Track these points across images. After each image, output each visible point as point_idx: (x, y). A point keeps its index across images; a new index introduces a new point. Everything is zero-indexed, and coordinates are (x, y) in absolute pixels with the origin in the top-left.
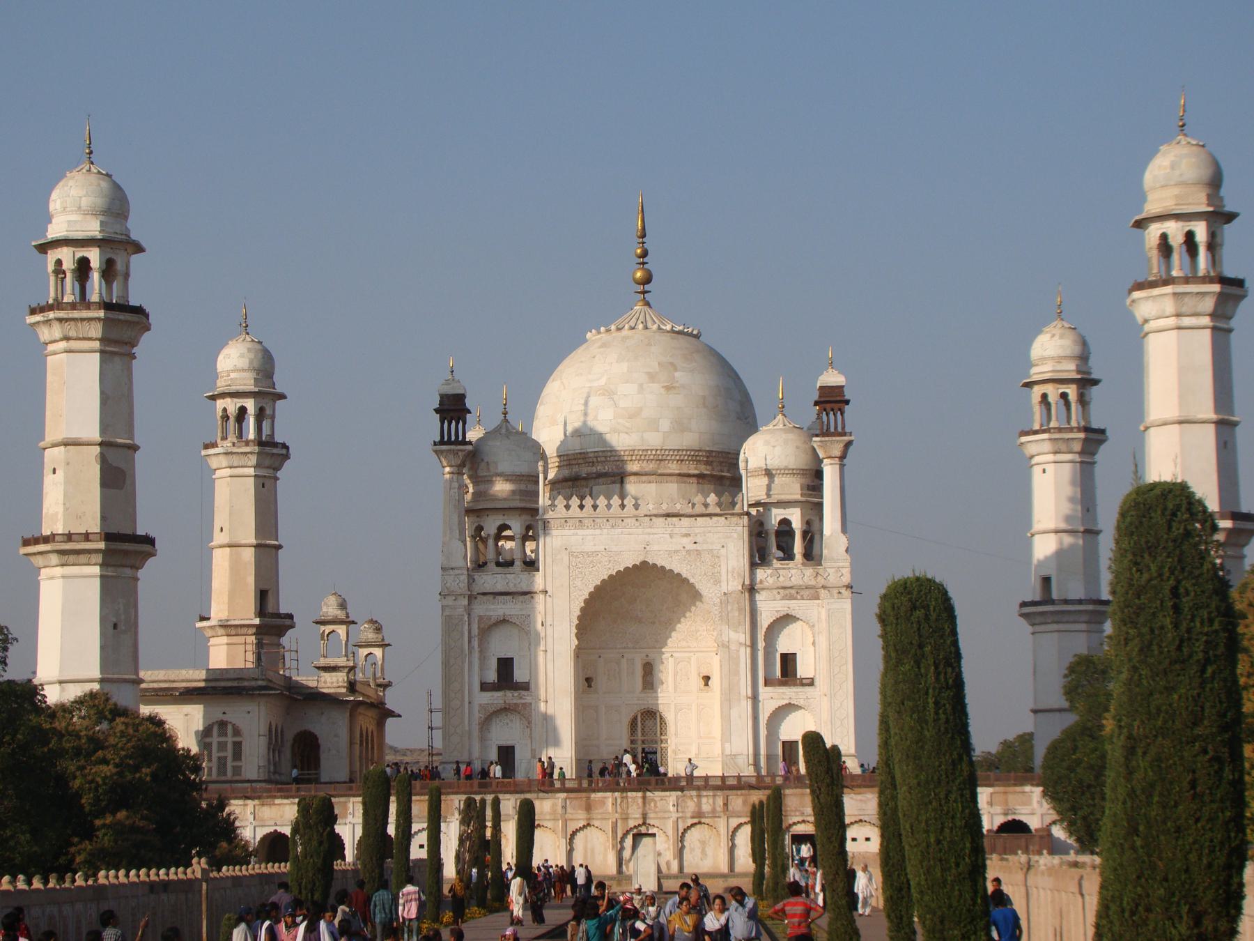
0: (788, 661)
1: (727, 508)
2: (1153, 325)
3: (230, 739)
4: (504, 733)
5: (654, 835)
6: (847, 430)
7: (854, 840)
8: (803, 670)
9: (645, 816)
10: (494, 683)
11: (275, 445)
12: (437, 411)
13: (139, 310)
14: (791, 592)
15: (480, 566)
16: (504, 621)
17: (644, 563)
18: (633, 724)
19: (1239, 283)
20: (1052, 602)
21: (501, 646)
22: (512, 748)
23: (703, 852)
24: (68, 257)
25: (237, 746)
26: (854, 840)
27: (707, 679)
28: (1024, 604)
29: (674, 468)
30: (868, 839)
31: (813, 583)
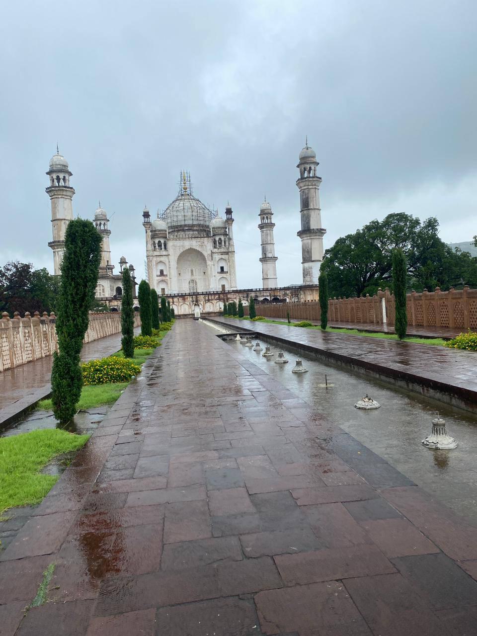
0: (222, 268)
1: (208, 236)
2: (302, 188)
3: (101, 288)
4: (163, 286)
9: (197, 301)
11: (108, 230)
13: (72, 188)
14: (222, 253)
15: (155, 250)
18: (190, 282)
19: (320, 178)
20: (266, 258)
21: (161, 267)
22: (164, 289)
23: (210, 308)
24: (55, 176)
25: (103, 289)
27: (204, 273)
28: (260, 259)
29: (195, 228)
31: (227, 251)
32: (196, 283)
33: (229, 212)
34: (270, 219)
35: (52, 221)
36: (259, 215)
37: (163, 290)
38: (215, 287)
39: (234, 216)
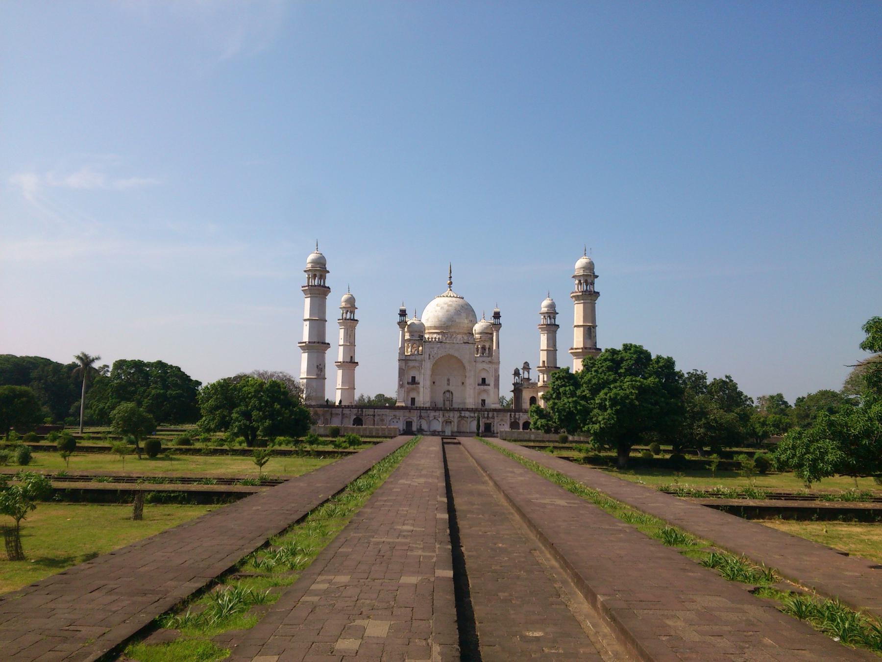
0: (484, 380)
8: (487, 382)
33: (497, 316)
39: (502, 320)
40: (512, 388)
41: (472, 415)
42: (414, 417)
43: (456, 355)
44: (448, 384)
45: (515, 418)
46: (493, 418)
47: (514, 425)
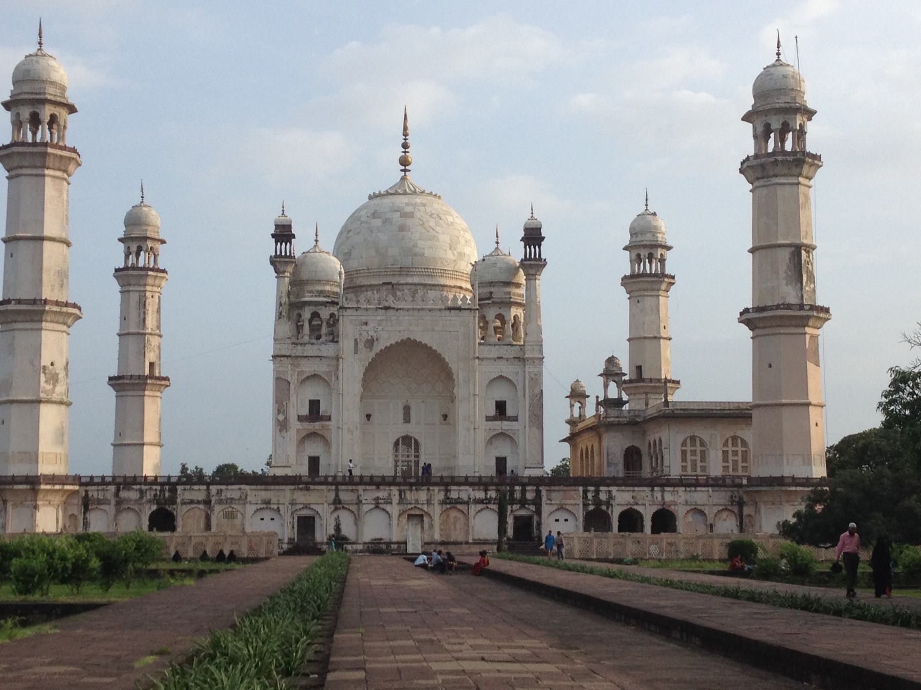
0: (501, 407)
4: (314, 449)
5: (422, 516)
6: (543, 257)
7: (557, 520)
8: (510, 412)
10: (306, 416)
12: (273, 236)
16: (315, 376)
17: (409, 339)
18: (396, 444)
21: (313, 392)
26: (557, 520)
27: (445, 417)
30: (566, 520)
32: (417, 443)
34: (662, 261)
35: (5, 241)
36: (625, 248)
37: (314, 462)
38: (473, 456)
39: (547, 250)
40: (566, 431)
41: (480, 495)
42: (318, 501)
43: (426, 339)
44: (407, 420)
45: (597, 502)
46: (537, 502)
47: (596, 519)
